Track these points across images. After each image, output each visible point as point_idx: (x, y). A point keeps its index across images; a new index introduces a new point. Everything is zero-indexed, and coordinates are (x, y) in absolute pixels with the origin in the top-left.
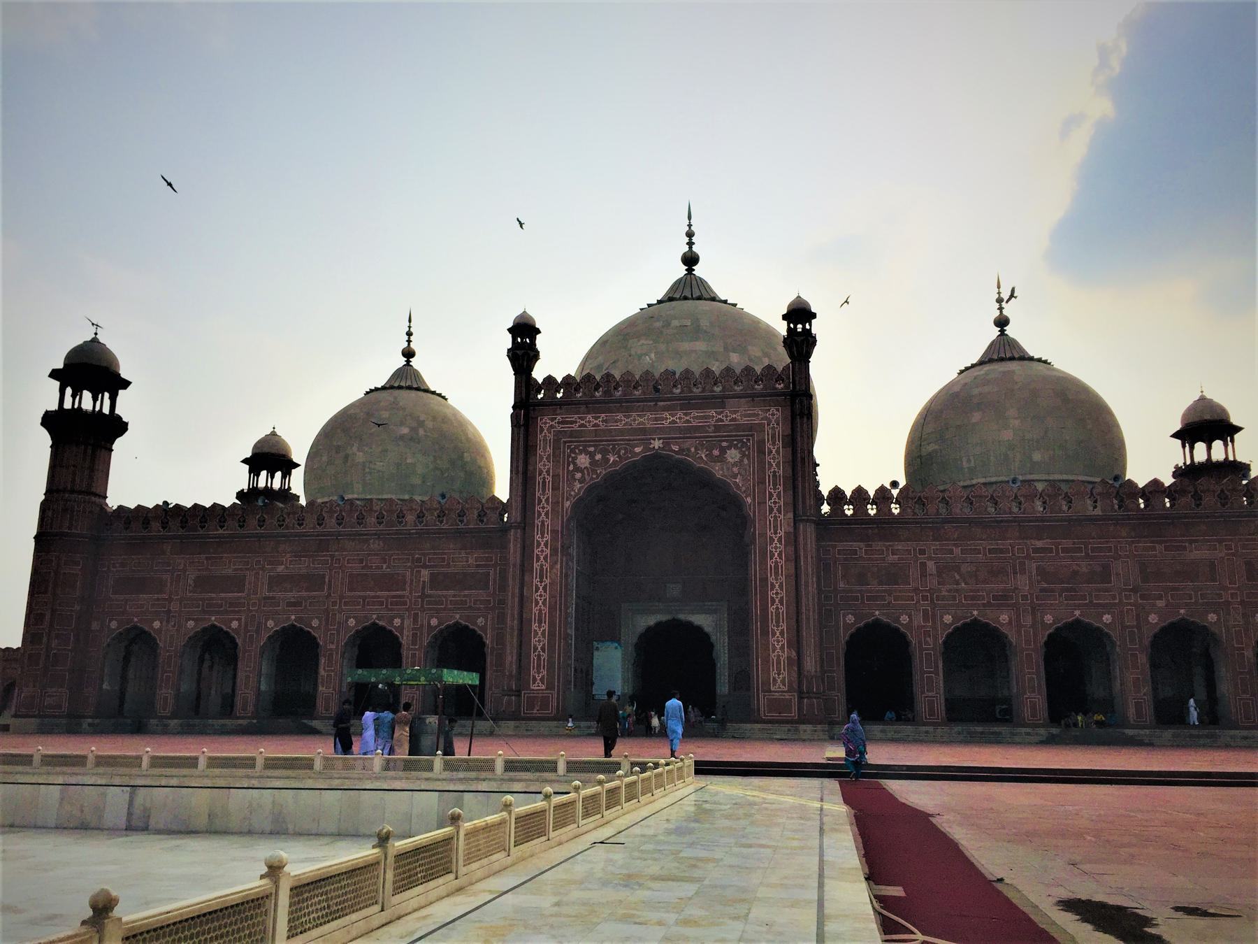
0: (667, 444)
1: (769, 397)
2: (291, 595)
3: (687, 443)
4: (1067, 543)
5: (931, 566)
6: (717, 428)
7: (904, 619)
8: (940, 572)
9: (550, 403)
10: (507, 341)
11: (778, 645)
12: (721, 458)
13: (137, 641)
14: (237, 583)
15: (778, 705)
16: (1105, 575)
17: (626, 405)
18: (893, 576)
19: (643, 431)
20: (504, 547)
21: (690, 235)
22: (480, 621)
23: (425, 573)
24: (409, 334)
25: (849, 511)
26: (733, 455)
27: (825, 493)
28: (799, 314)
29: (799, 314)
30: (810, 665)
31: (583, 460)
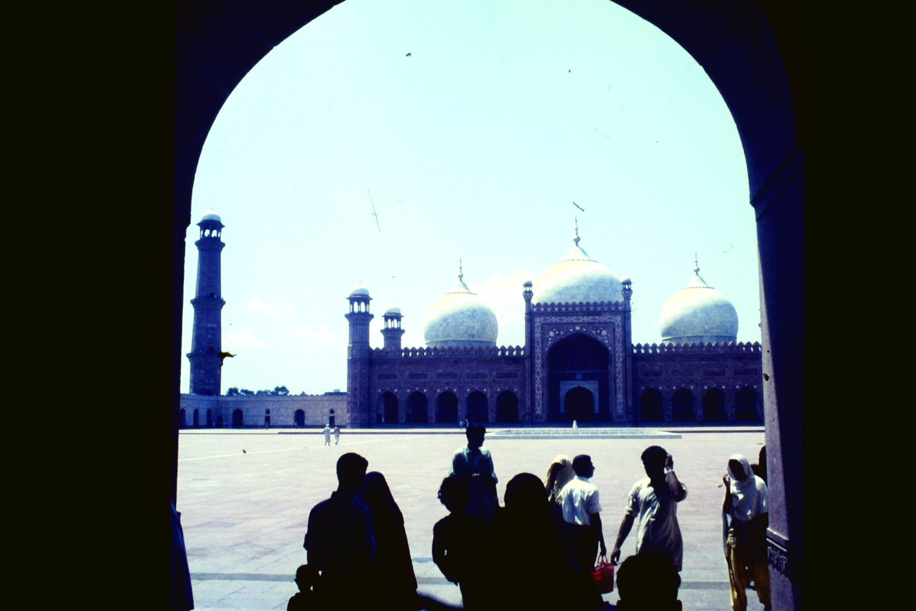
0: (581, 329)
1: (617, 312)
2: (446, 381)
4: (713, 363)
5: (670, 370)
6: (600, 323)
9: (539, 314)
10: (523, 289)
11: (620, 397)
12: (600, 334)
13: (389, 398)
14: (425, 376)
15: (619, 417)
17: (567, 314)
18: (658, 374)
20: (524, 364)
21: (577, 229)
22: (515, 390)
23: (494, 373)
25: (643, 351)
27: (635, 345)
28: (628, 283)
29: (628, 283)
30: (630, 403)
31: (552, 334)
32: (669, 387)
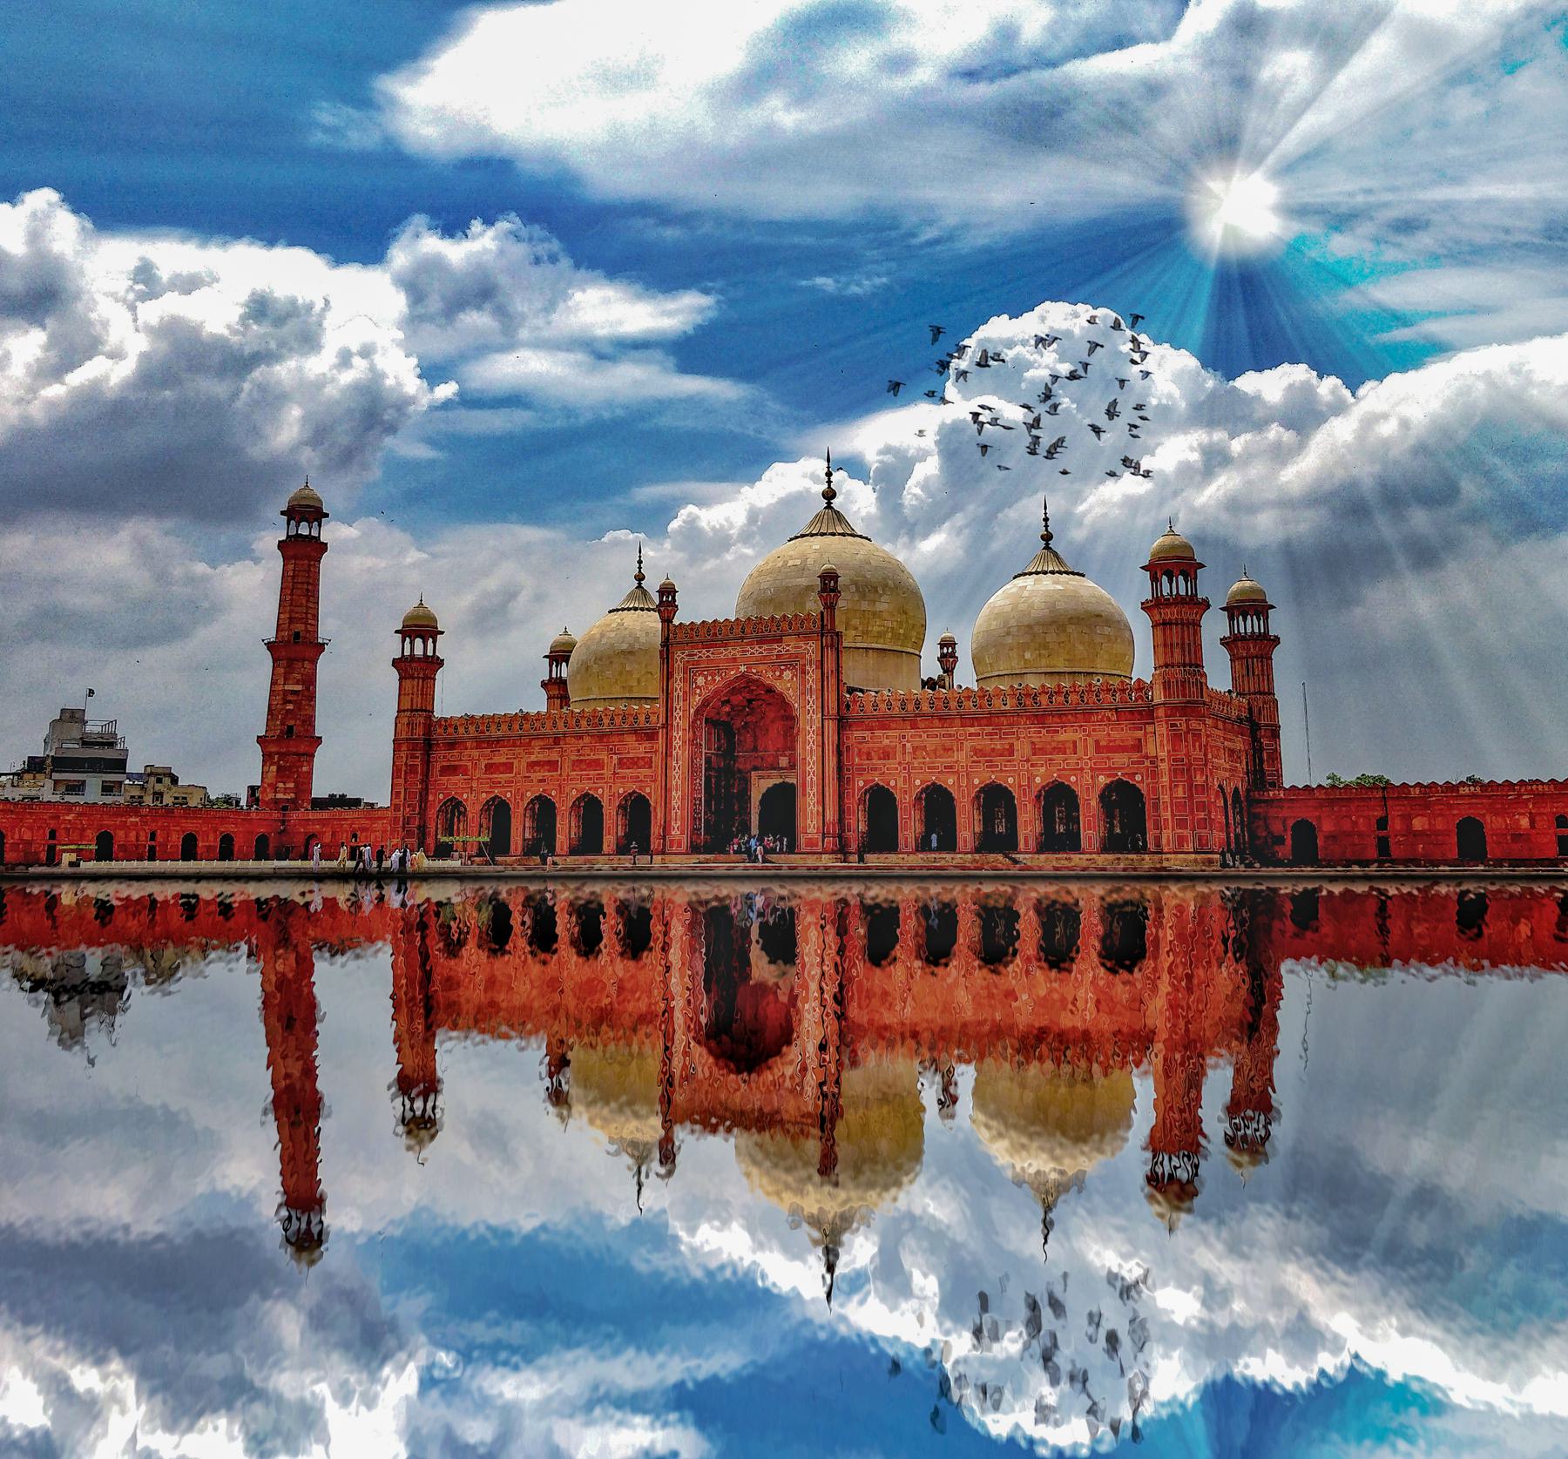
2: (539, 775)
3: (761, 667)
4: (989, 729)
5: (908, 745)
6: (778, 656)
7: (892, 783)
8: (915, 749)
14: (508, 767)
15: (810, 843)
16: (1011, 752)
18: (886, 755)
19: (735, 660)
24: (640, 562)
26: (787, 674)
30: (831, 815)
31: (701, 681)
32: (908, 780)
